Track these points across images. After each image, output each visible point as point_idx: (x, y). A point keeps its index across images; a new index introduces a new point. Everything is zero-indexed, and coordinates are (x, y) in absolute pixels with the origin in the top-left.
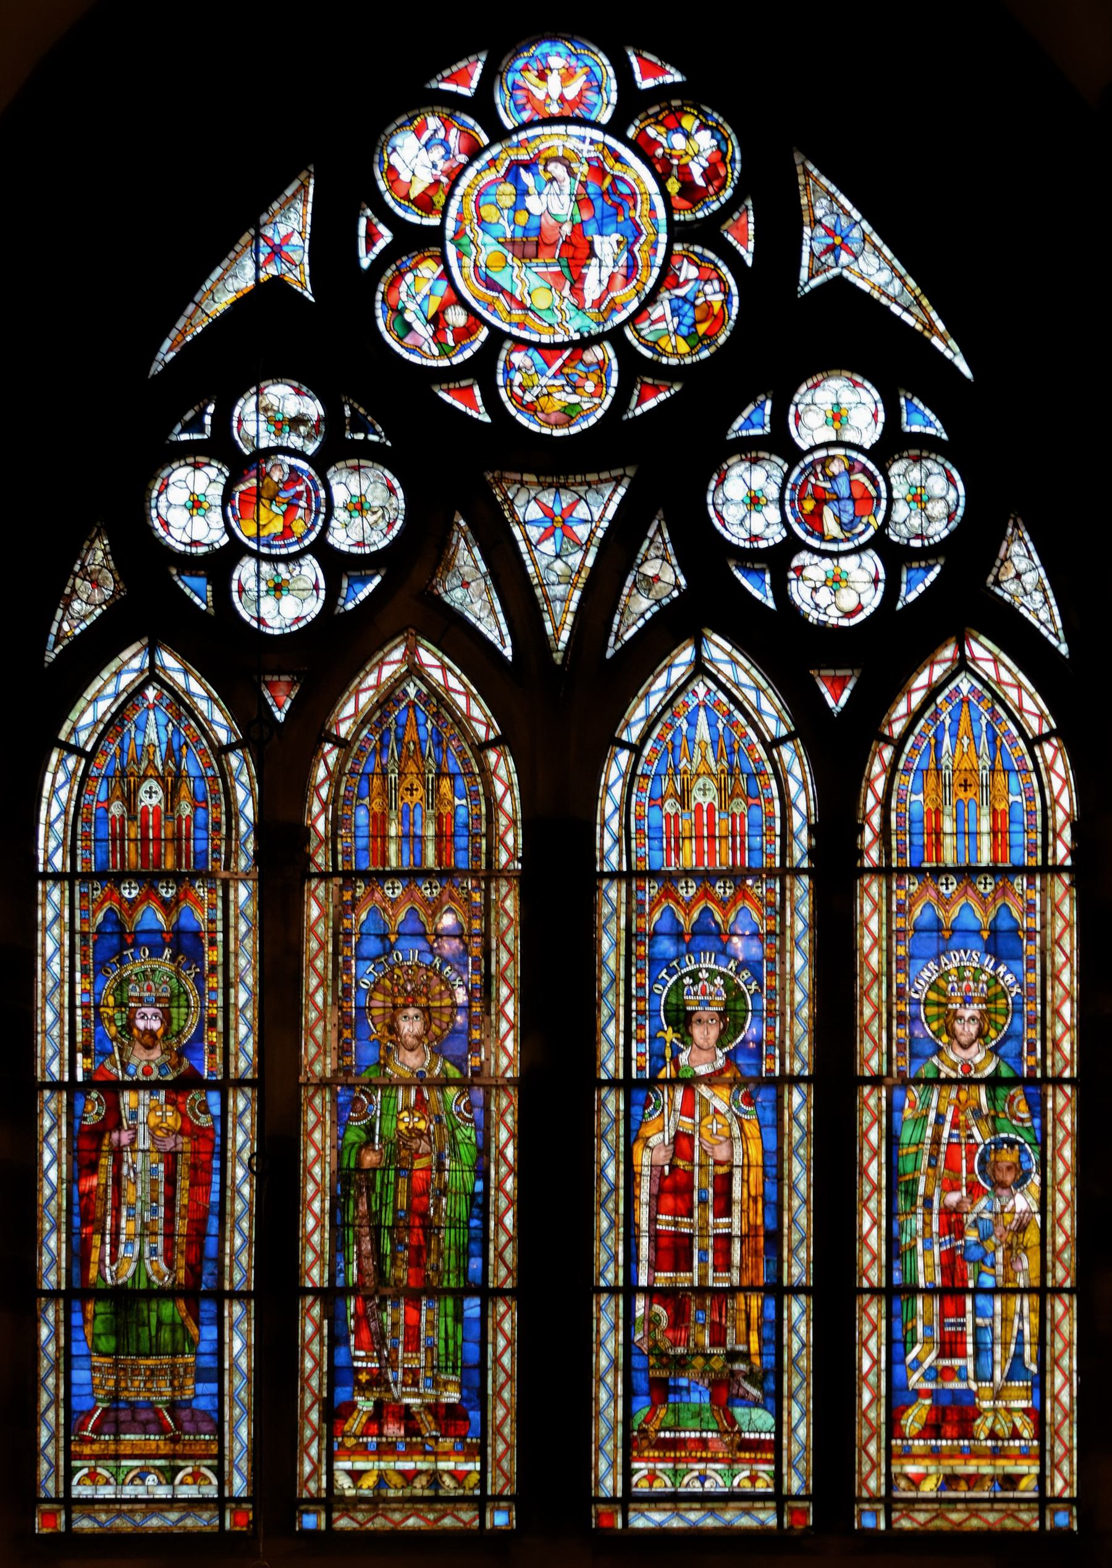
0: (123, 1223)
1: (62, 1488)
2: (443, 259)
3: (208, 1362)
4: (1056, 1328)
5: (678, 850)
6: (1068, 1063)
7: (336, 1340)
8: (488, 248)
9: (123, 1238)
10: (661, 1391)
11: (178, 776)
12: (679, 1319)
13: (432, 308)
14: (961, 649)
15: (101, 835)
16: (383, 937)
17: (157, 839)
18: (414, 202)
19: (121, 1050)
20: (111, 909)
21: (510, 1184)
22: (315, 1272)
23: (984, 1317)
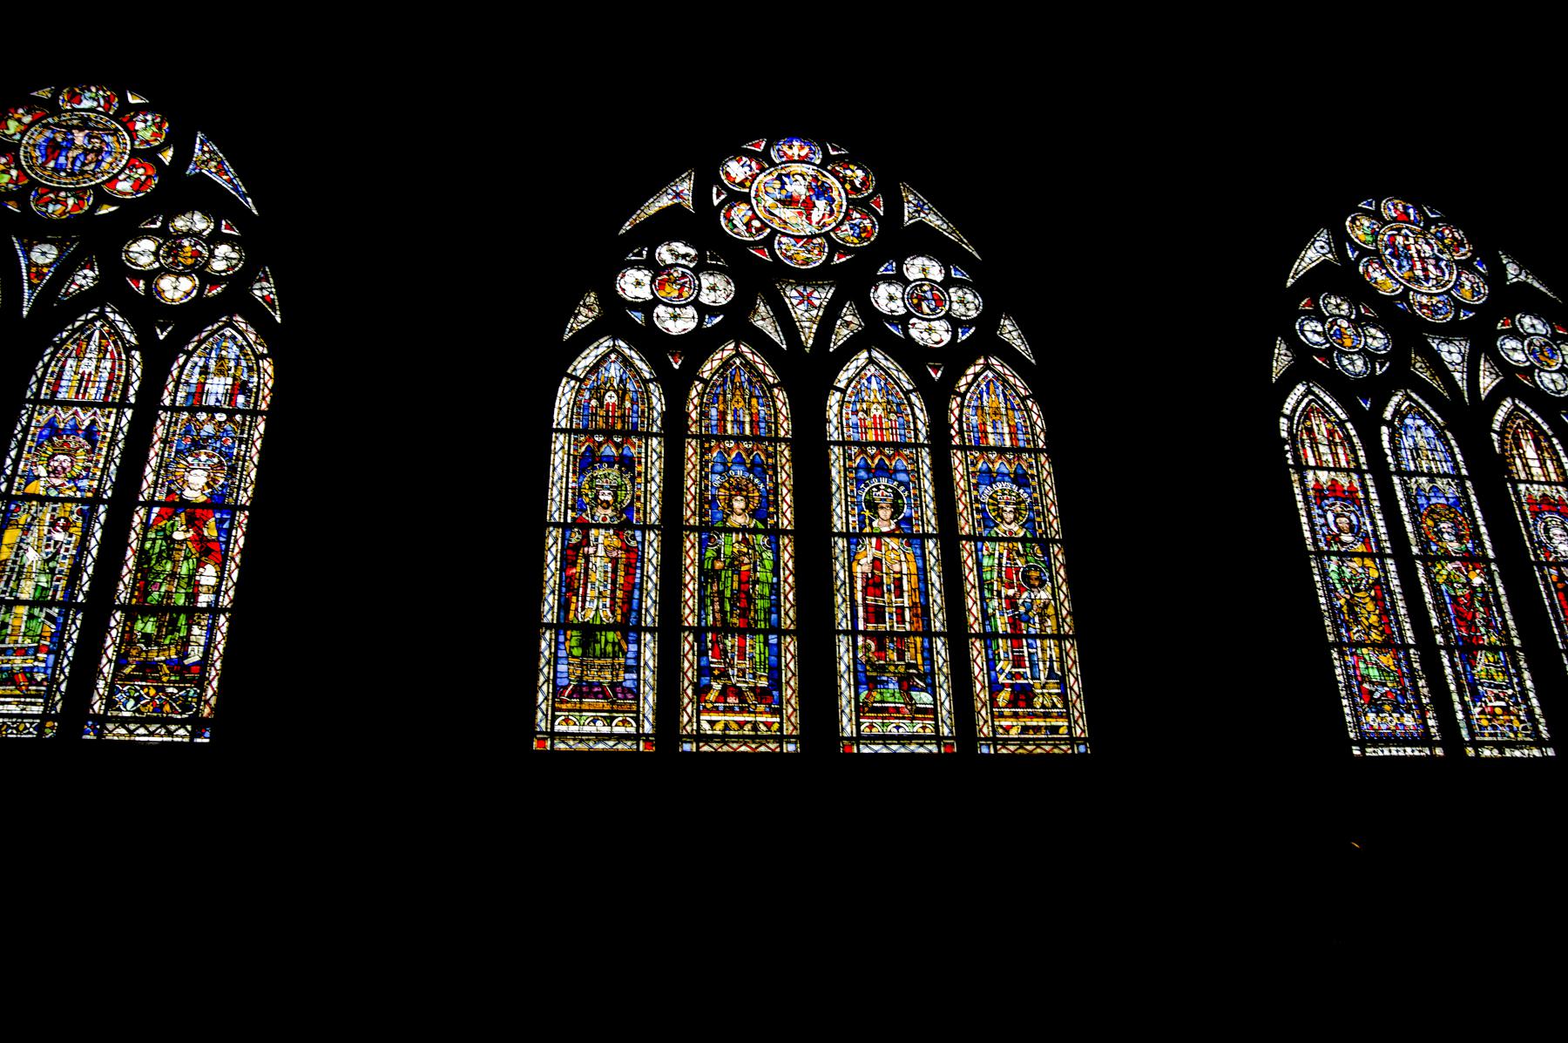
0: (589, 591)
1: (549, 726)
2: (749, 203)
3: (631, 662)
4: (1067, 654)
5: (866, 433)
6: (1057, 533)
7: (702, 653)
8: (769, 202)
9: (588, 599)
10: (873, 684)
11: (625, 391)
12: (881, 648)
13: (745, 220)
14: (986, 359)
15: (586, 413)
16: (724, 464)
17: (613, 417)
18: (739, 184)
19: (591, 509)
20: (589, 446)
21: (791, 580)
22: (690, 619)
23: (1033, 648)
